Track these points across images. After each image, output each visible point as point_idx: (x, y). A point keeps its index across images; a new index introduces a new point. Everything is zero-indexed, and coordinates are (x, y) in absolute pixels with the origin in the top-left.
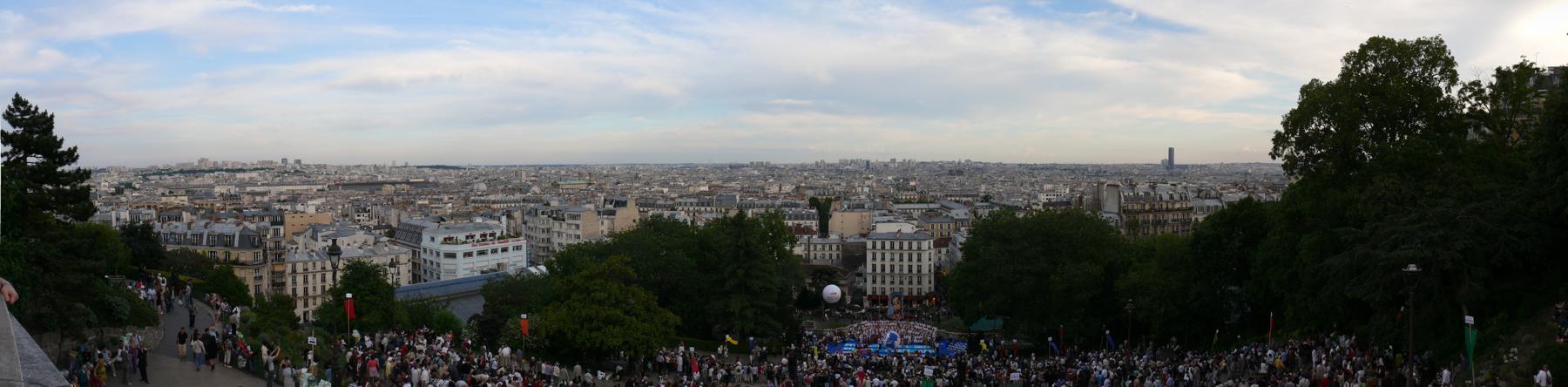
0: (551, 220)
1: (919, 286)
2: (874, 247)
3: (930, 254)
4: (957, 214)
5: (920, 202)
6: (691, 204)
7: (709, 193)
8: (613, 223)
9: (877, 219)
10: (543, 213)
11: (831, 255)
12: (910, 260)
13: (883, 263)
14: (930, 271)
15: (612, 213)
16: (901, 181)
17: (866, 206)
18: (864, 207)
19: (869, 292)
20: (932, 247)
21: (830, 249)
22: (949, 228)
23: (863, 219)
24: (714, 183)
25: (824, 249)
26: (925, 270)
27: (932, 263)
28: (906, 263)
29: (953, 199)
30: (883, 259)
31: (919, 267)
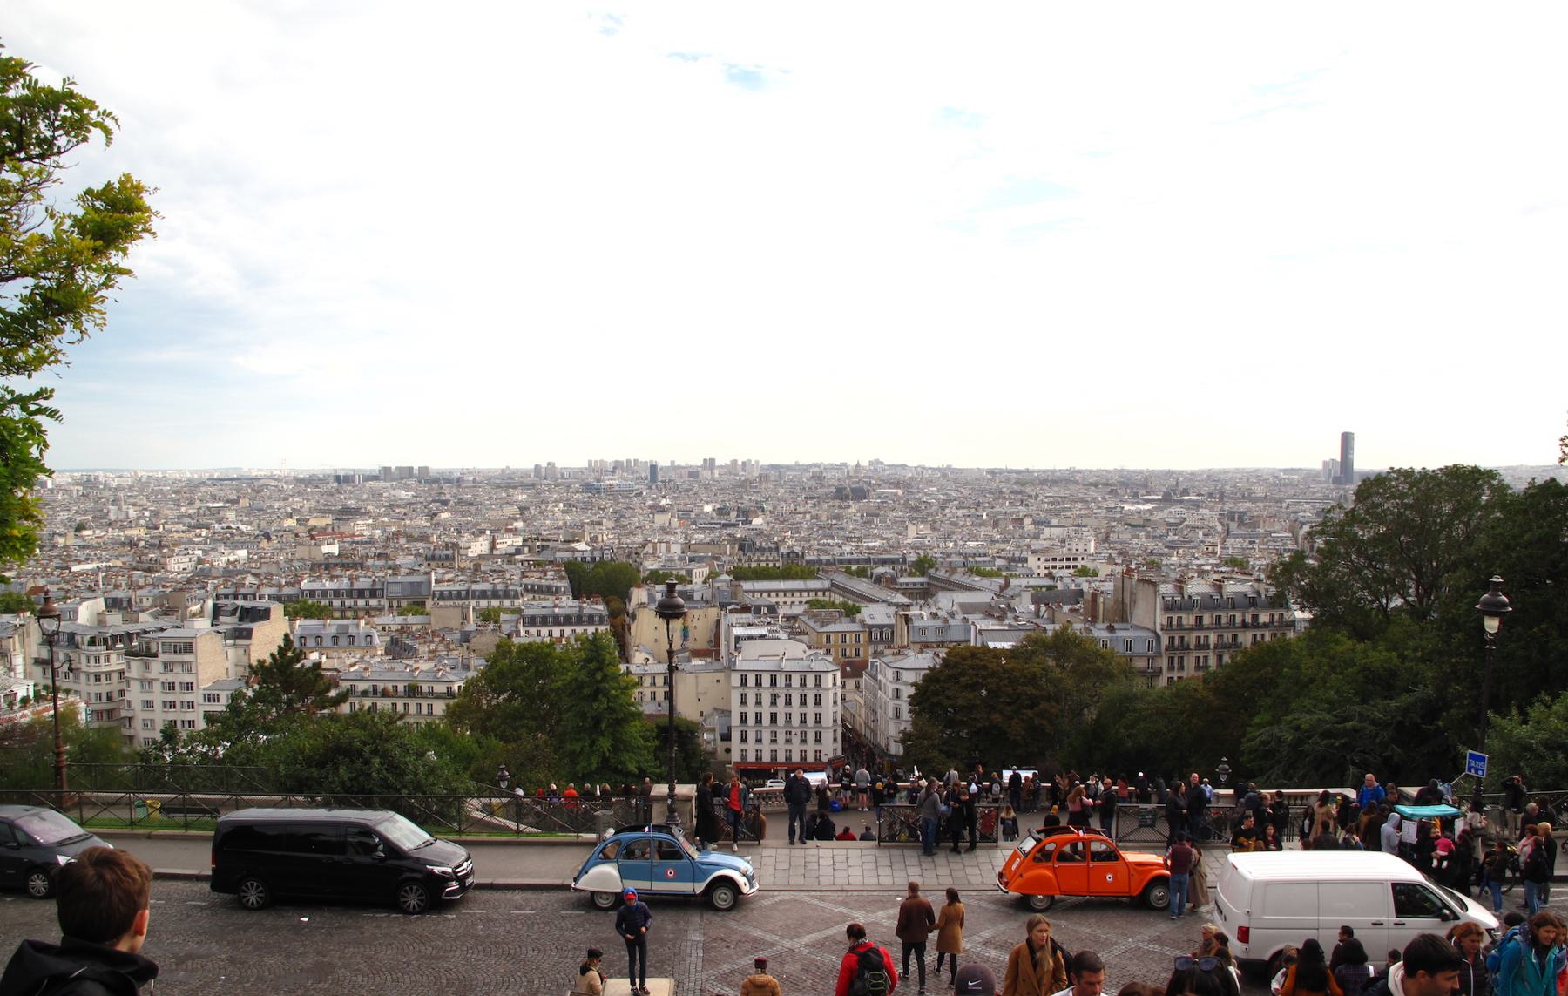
0: (113, 657)
1: (818, 747)
2: (744, 682)
3: (835, 694)
6: (336, 593)
7: (345, 562)
9: (738, 631)
10: (93, 642)
12: (803, 703)
13: (759, 710)
14: (835, 721)
15: (248, 634)
16: (733, 514)
17: (697, 596)
19: (736, 757)
21: (653, 683)
22: (858, 641)
24: (313, 522)
26: (827, 720)
27: (839, 708)
28: (796, 710)
29: (854, 567)
30: (759, 703)
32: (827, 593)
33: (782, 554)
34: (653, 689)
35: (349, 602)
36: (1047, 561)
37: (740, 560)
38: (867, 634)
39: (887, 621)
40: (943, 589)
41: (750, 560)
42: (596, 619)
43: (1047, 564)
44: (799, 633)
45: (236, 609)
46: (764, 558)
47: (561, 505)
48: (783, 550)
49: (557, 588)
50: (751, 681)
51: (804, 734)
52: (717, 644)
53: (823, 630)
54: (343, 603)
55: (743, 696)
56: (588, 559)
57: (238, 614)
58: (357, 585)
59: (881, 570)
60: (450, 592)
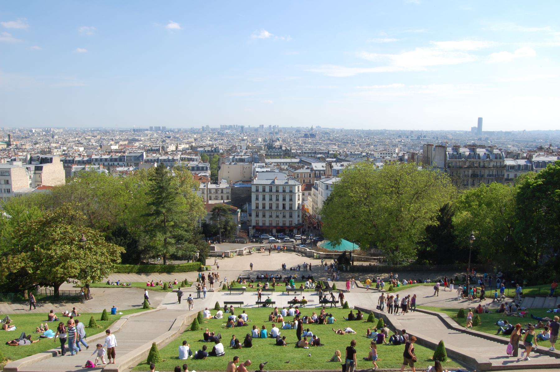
1: (291, 219)
3: (299, 195)
4: (316, 167)
8: (40, 177)
9: (257, 170)
13: (264, 202)
15: (40, 169)
18: (245, 161)
20: (300, 191)
21: (222, 192)
22: (310, 177)
23: (245, 170)
24: (121, 143)
25: (217, 192)
29: (310, 155)
30: (264, 199)
33: (283, 150)
34: (222, 195)
35: (110, 163)
36: (381, 154)
37: (267, 152)
39: (322, 169)
41: (271, 152)
42: (205, 168)
43: (381, 155)
44: (284, 170)
45: (39, 158)
46: (276, 151)
47: (209, 138)
48: (284, 148)
49: (194, 159)
50: (261, 189)
53: (295, 172)
54: (109, 164)
57: (40, 161)
58: (114, 157)
59: (320, 156)
60: (151, 160)
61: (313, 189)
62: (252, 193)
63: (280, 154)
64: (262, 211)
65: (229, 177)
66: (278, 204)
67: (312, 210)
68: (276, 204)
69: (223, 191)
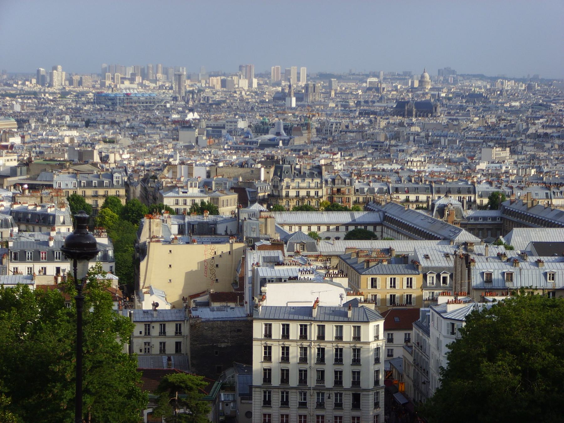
1: (356, 413)
2: (268, 335)
4: (427, 257)
5: (332, 207)
11: (163, 345)
14: (377, 382)
17: (221, 229)
21: (163, 332)
25: (148, 333)
26: (367, 382)
27: (382, 367)
29: (412, 197)
31: (356, 375)
32: (379, 228)
33: (326, 181)
34: (162, 339)
38: (421, 276)
40: (520, 225)
47: (67, 118)
51: (339, 395)
52: (242, 288)
55: (268, 350)
56: (95, 182)
61: (414, 328)
62: (254, 343)
63: (317, 193)
64: (280, 390)
65: (170, 280)
66: (323, 372)
67: (413, 388)
68: (317, 371)
69: (166, 331)
